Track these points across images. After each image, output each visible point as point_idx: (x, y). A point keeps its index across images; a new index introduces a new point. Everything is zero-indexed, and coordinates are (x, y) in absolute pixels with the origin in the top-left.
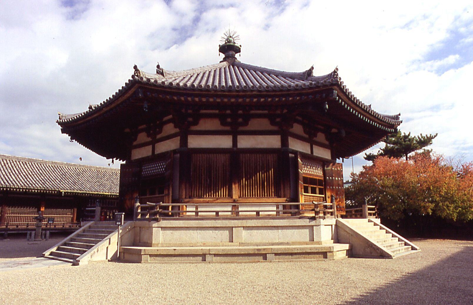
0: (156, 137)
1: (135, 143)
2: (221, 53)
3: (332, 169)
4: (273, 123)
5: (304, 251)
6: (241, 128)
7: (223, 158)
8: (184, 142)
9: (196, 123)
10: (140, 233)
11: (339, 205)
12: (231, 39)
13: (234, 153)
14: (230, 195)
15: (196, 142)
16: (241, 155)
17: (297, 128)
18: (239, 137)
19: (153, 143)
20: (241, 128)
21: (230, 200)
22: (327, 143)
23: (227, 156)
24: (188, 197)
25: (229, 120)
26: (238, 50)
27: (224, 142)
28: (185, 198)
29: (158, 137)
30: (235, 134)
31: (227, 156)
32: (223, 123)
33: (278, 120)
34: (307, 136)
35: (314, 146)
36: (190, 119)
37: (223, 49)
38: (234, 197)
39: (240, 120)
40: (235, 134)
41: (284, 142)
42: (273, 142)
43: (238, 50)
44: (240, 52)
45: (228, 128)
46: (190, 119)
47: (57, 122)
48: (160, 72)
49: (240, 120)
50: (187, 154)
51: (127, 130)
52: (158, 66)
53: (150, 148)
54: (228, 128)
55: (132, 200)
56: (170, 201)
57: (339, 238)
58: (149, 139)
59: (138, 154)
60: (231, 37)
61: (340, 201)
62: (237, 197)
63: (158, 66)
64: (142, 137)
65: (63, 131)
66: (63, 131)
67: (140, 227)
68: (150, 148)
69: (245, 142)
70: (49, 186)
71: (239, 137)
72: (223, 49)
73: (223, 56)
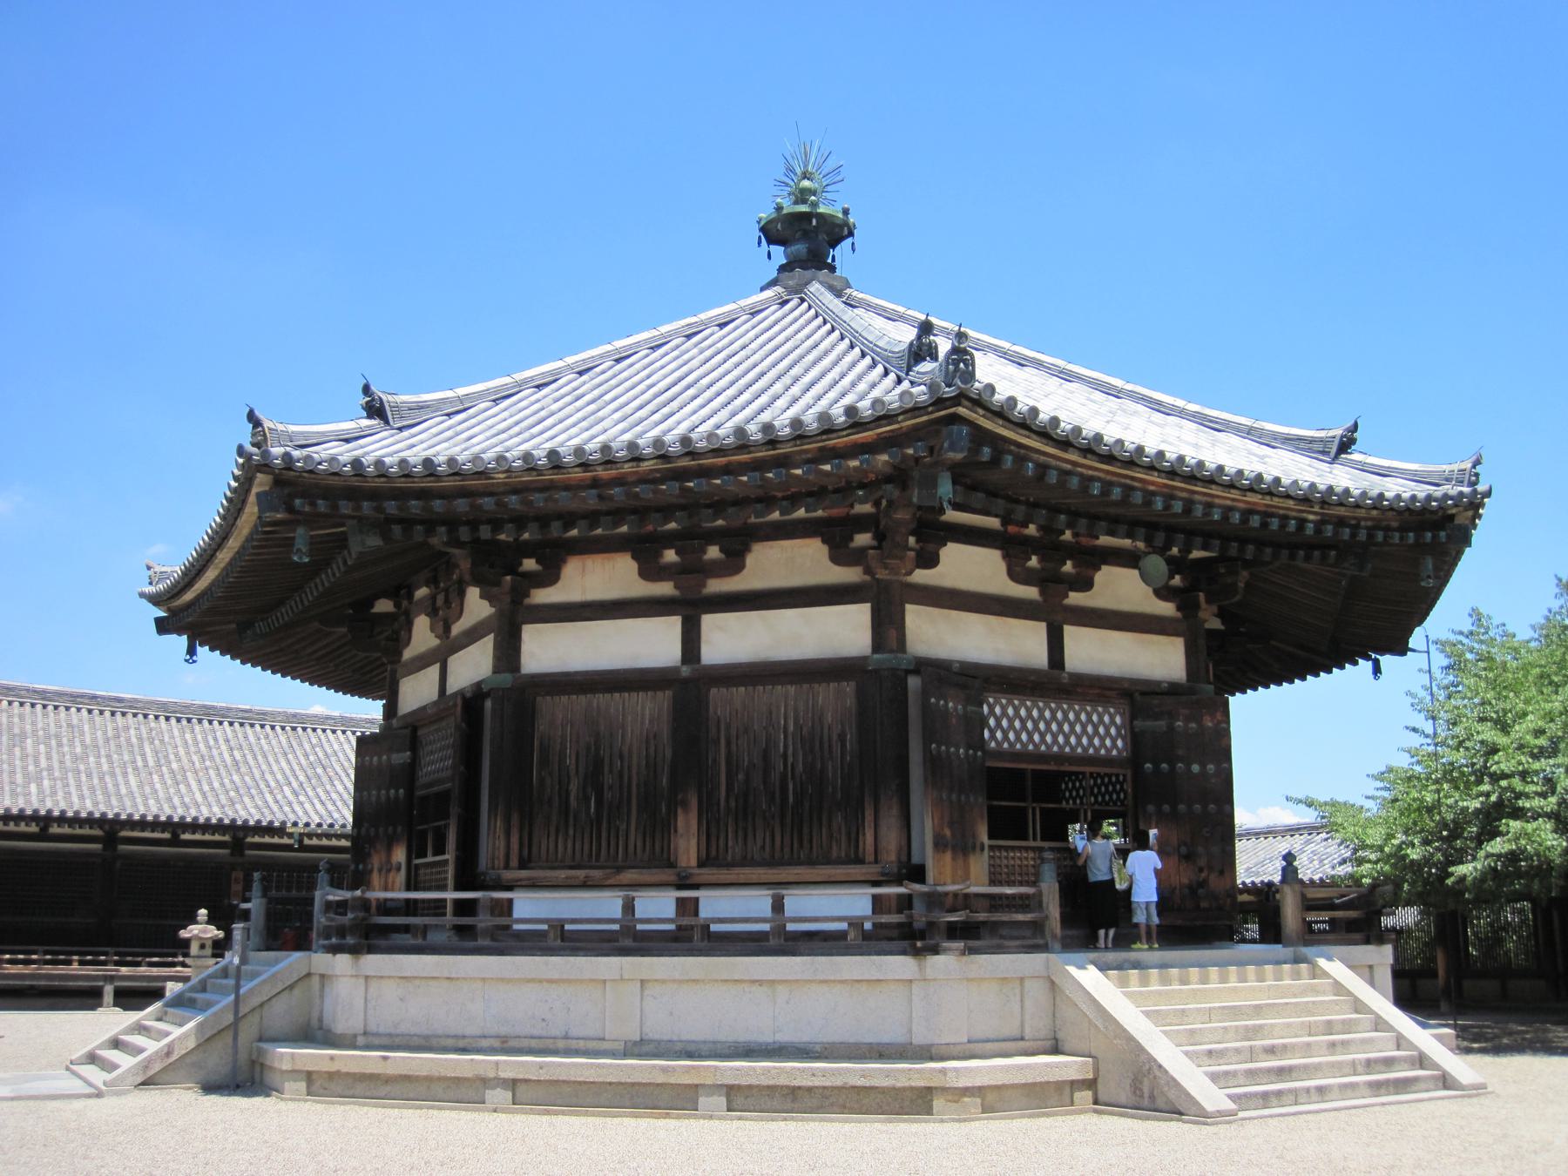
0: (447, 629)
1: (408, 654)
2: (773, 248)
3: (1171, 728)
4: (841, 554)
5: (839, 1083)
6: (716, 586)
7: (649, 709)
8: (508, 653)
9: (550, 576)
10: (322, 997)
11: (1203, 884)
12: (806, 183)
13: (690, 686)
14: (666, 860)
15: (549, 650)
16: (714, 691)
17: (969, 566)
18: (709, 621)
19: (440, 657)
20: (716, 586)
21: (668, 875)
22: (1167, 609)
23: (664, 698)
24: (514, 862)
25: (670, 556)
26: (837, 231)
27: (653, 643)
28: (507, 867)
29: (456, 629)
30: (691, 609)
31: (664, 698)
32: (650, 571)
33: (863, 539)
34: (1031, 592)
35: (1069, 630)
36: (530, 564)
37: (772, 233)
38: (682, 862)
39: (713, 552)
40: (691, 609)
41: (887, 626)
42: (843, 631)
43: (837, 231)
44: (851, 234)
45: (665, 589)
46: (530, 564)
47: (142, 595)
48: (375, 410)
49: (713, 552)
50: (518, 698)
51: (384, 606)
52: (366, 390)
53: (434, 671)
54: (665, 589)
55: (389, 871)
56: (450, 882)
57: (1060, 1035)
58: (433, 642)
59: (418, 691)
60: (805, 176)
61: (1211, 869)
62: (694, 862)
63: (366, 390)
64: (422, 636)
65: (163, 627)
66: (163, 627)
67: (322, 976)
68: (434, 671)
69: (732, 639)
70: (248, 811)
71: (709, 621)
72: (772, 233)
73: (779, 254)
